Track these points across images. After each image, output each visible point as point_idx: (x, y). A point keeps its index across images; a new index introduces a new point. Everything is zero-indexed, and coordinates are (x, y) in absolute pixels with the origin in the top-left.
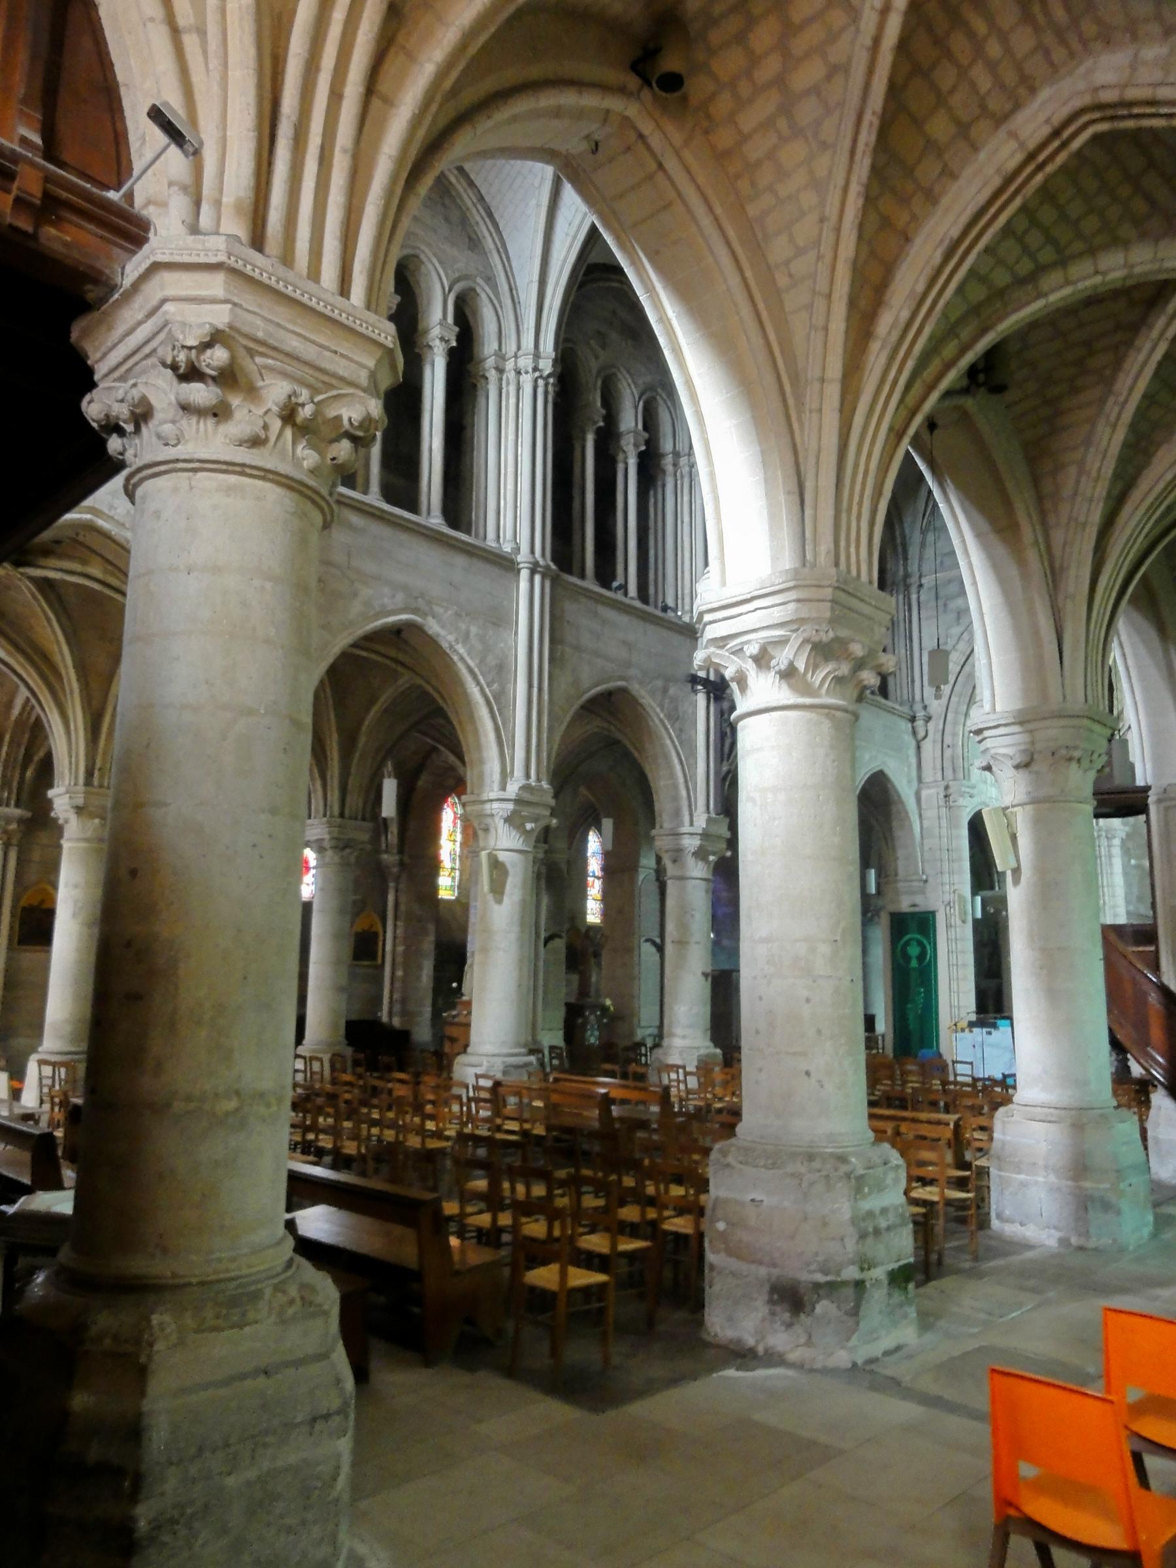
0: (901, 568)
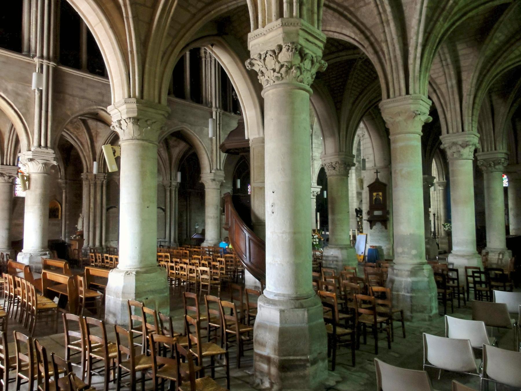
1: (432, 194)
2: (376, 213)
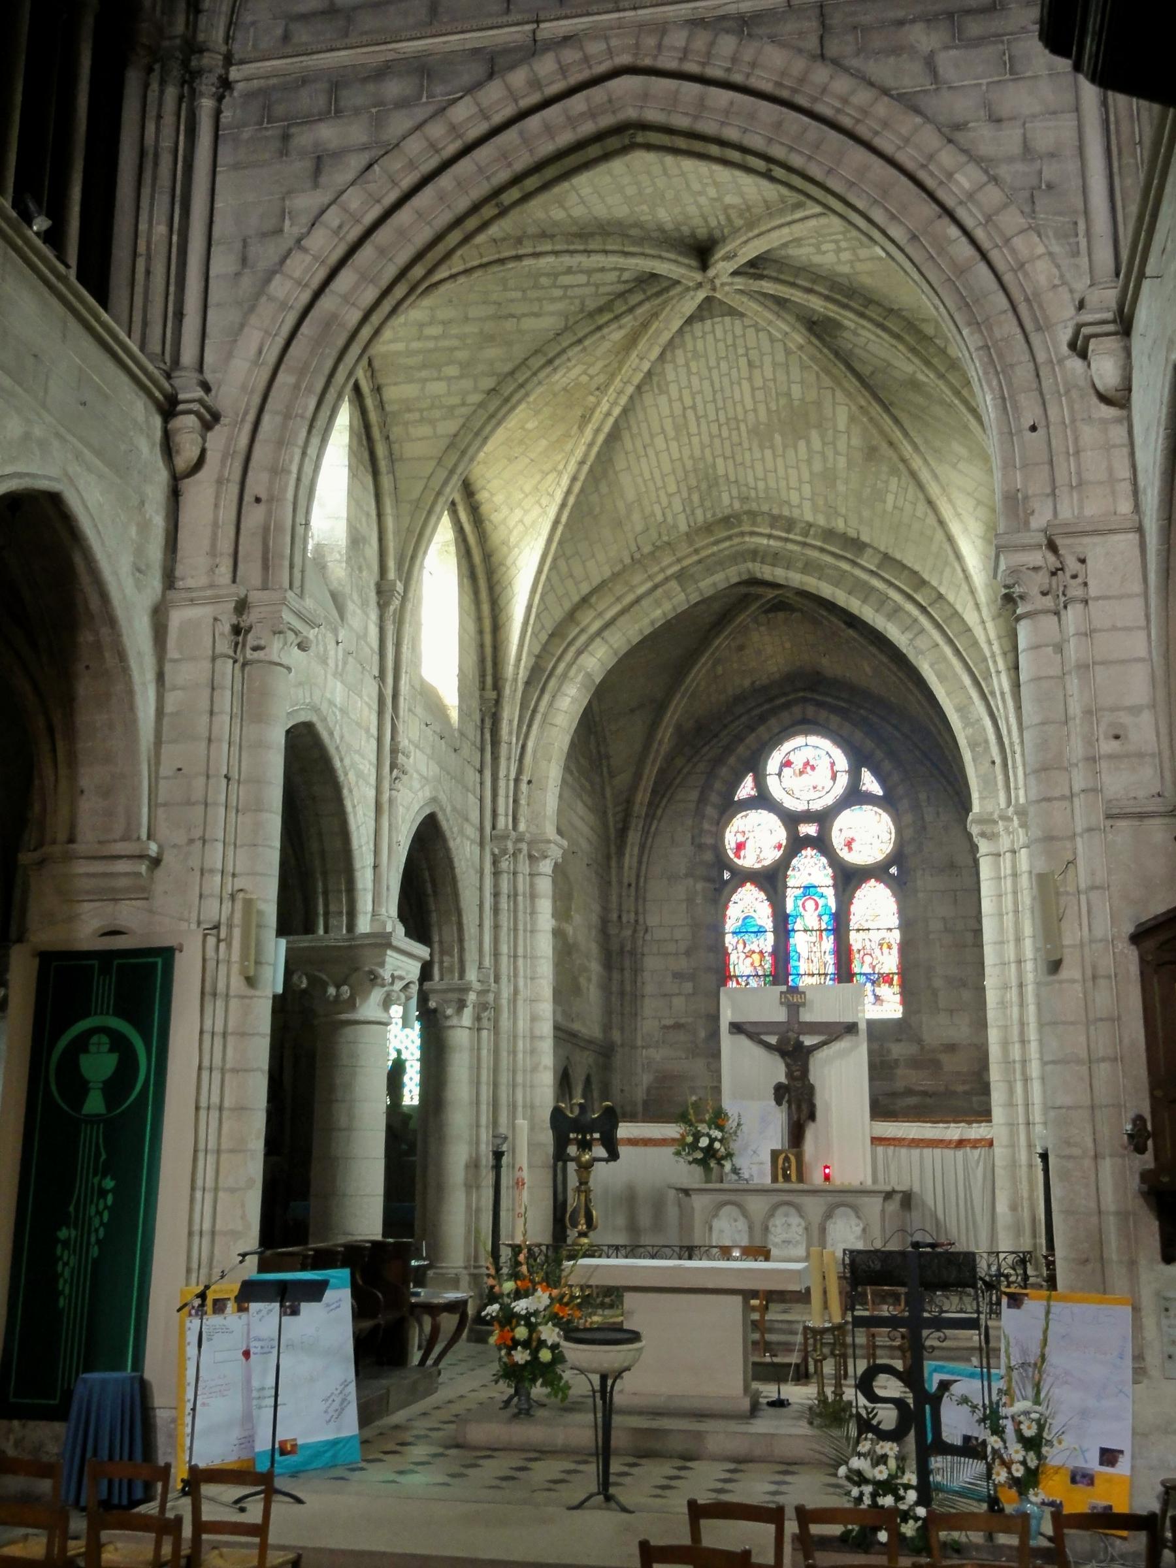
0: (180, 20)
1: (1005, 1044)
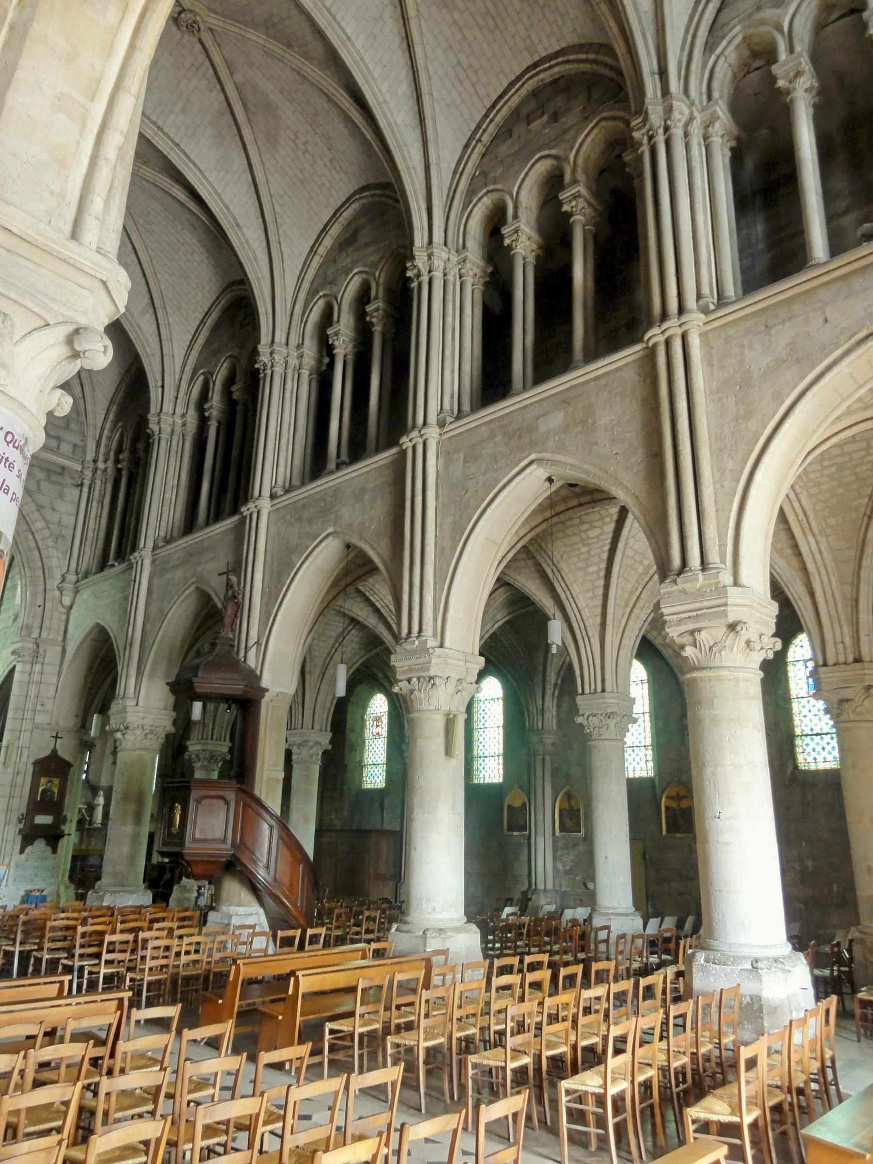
2: (42, 819)
